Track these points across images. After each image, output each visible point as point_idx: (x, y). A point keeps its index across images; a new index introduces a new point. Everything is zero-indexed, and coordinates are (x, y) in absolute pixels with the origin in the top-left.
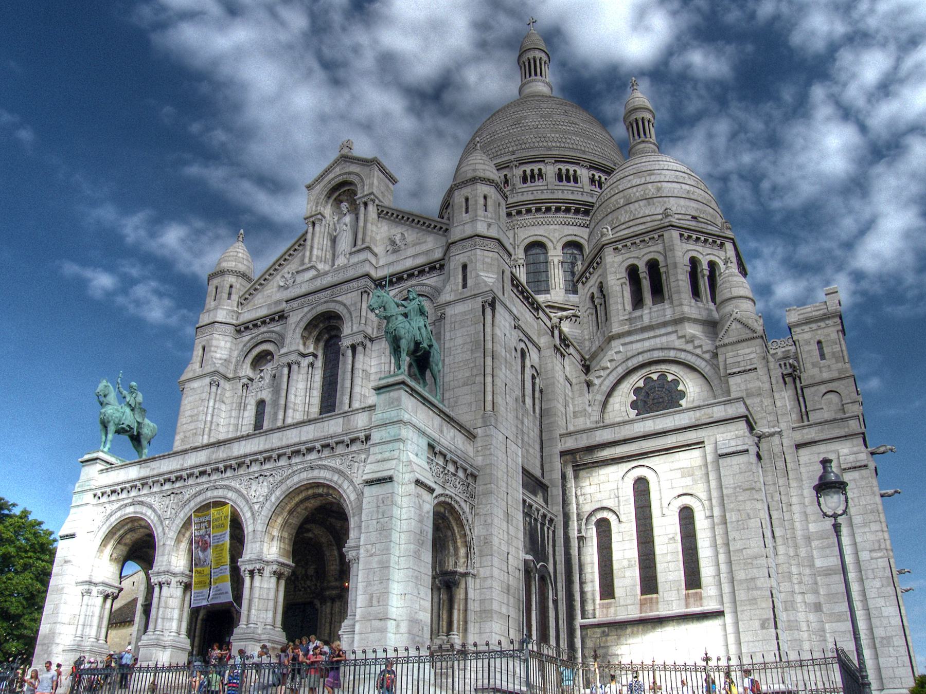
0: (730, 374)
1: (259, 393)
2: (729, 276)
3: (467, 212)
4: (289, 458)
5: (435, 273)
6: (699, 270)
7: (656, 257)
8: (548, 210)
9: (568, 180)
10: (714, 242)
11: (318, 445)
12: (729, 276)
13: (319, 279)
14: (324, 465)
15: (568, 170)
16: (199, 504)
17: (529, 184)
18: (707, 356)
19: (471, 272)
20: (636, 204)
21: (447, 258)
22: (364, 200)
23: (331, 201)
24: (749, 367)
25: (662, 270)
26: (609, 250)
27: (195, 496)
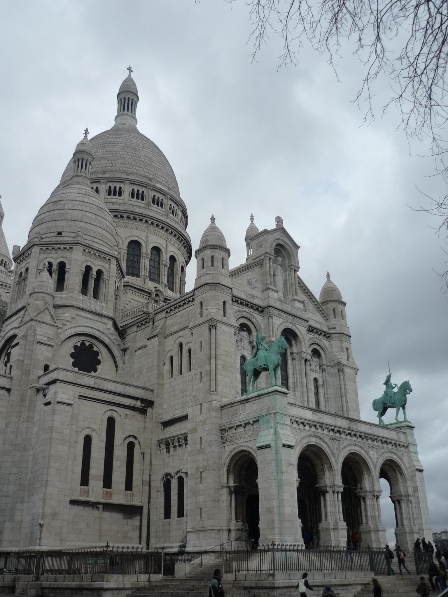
1: (243, 350)
4: (383, 443)
5: (325, 338)
11: (393, 442)
13: (285, 305)
21: (332, 335)
22: (296, 269)
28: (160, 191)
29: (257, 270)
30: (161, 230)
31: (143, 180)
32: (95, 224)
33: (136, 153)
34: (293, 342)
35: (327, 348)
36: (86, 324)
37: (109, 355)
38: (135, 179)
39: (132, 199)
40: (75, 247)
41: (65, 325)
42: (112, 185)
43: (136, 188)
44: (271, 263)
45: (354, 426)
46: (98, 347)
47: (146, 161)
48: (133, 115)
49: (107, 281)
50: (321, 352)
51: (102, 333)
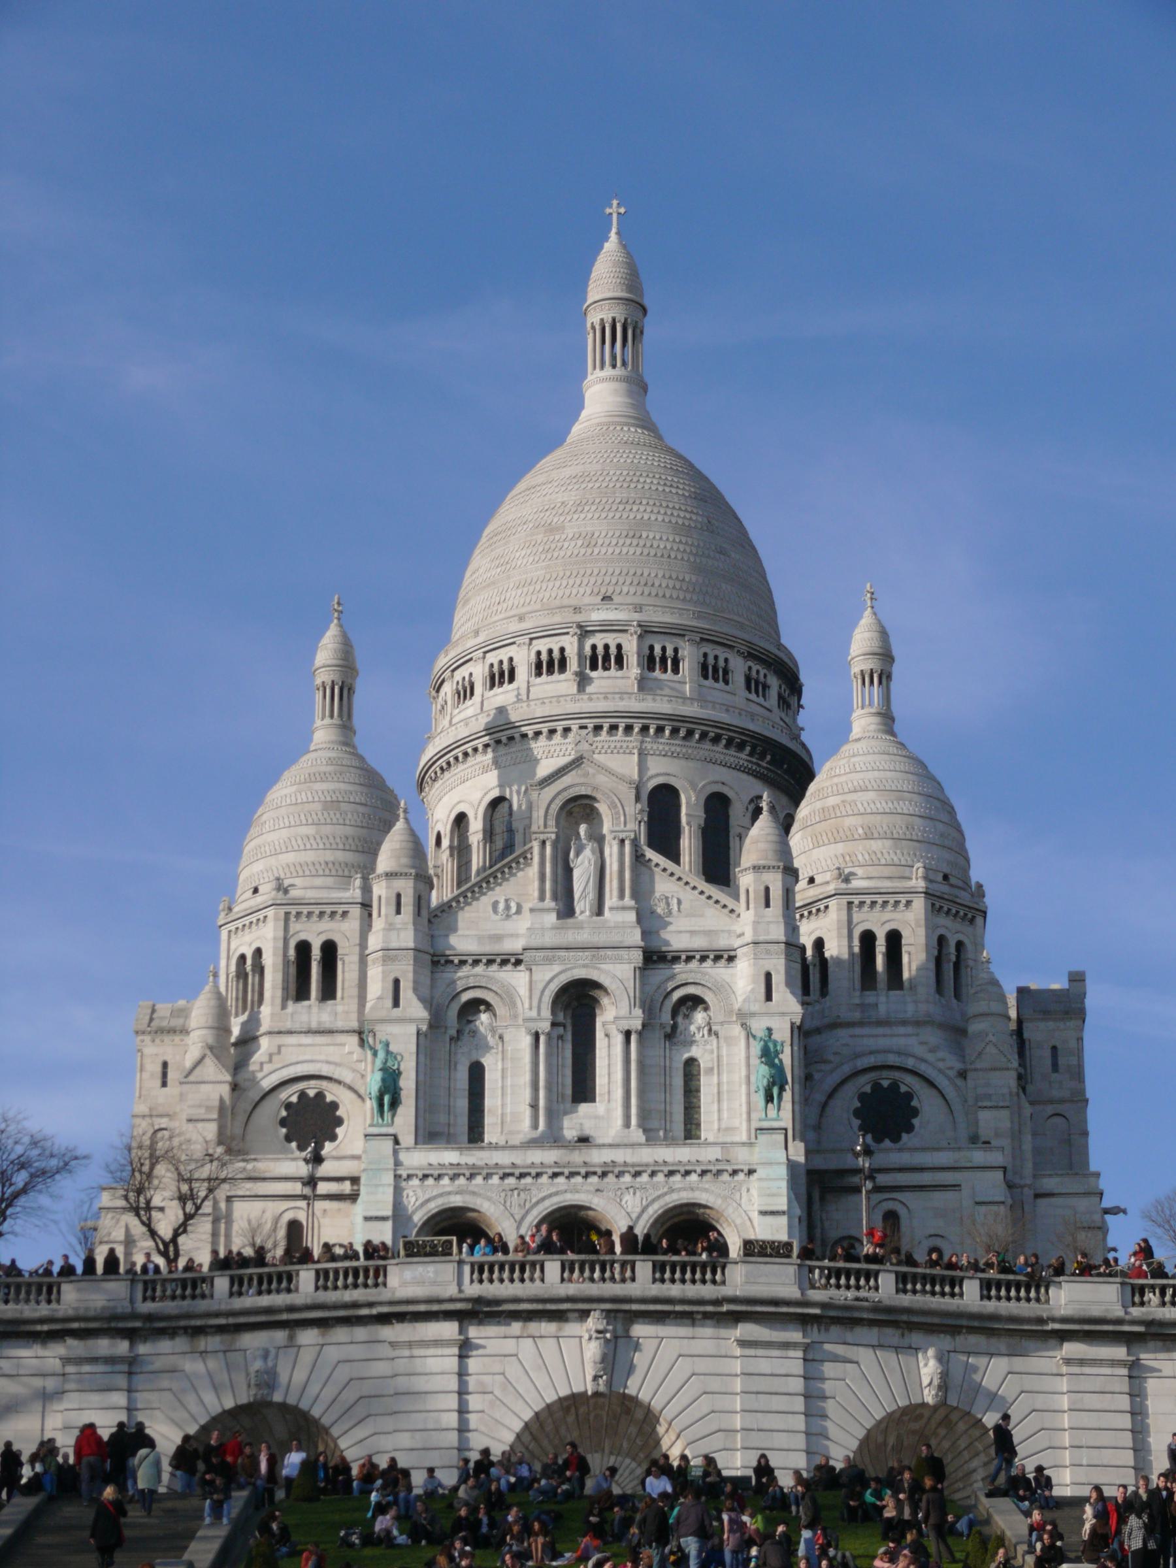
3: (767, 905)
6: (944, 951)
7: (900, 929)
8: (690, 733)
9: (716, 680)
10: (966, 915)
13: (570, 932)
15: (716, 657)
17: (657, 673)
18: (951, 1073)
19: (777, 984)
20: (880, 842)
21: (739, 952)
22: (622, 835)
24: (1001, 1104)
25: (904, 949)
27: (550, 1196)
28: (607, 628)
29: (520, 874)
31: (557, 619)
32: (315, 846)
34: (605, 1001)
36: (301, 1058)
37: (359, 1100)
38: (536, 625)
39: (539, 680)
42: (493, 658)
45: (577, 1157)
46: (333, 1093)
47: (576, 552)
49: (346, 958)
50: (708, 997)
51: (336, 1064)
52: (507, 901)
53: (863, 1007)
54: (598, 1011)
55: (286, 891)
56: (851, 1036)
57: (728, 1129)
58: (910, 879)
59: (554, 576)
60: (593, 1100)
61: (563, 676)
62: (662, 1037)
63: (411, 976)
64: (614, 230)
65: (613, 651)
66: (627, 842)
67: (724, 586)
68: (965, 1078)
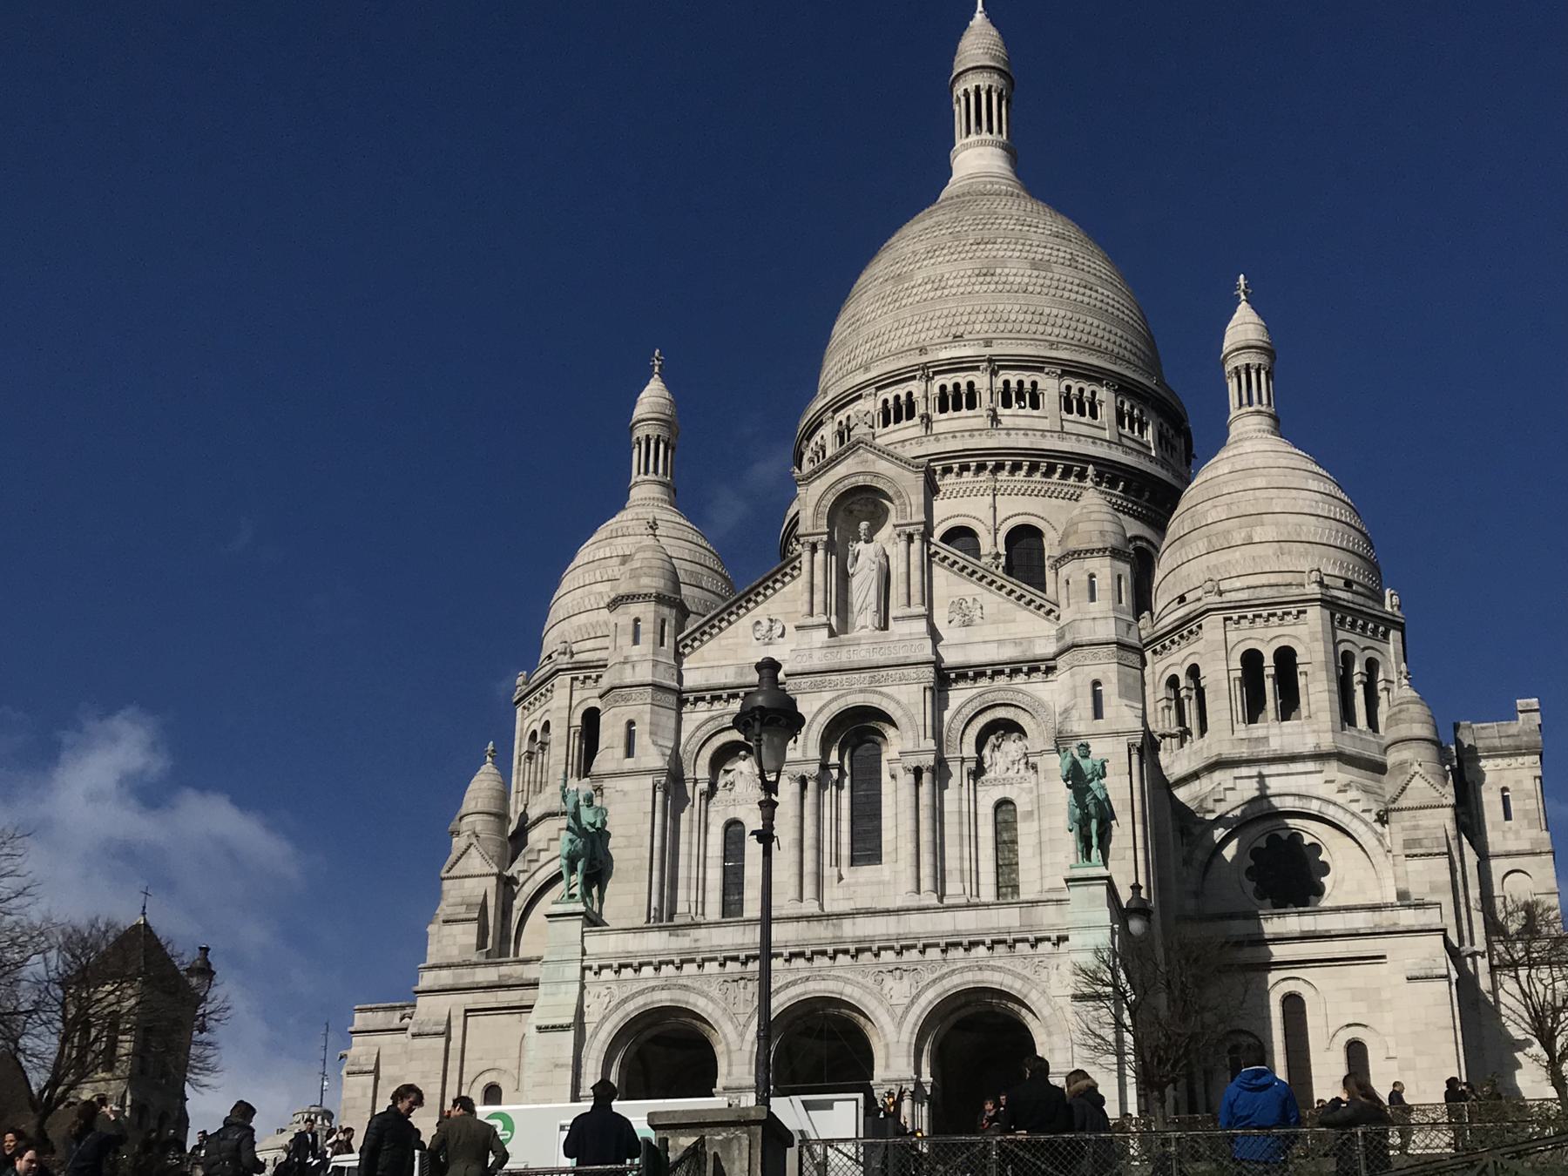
0: (1407, 856)
2: (1408, 702)
3: (1093, 599)
9: (1082, 413)
10: (1376, 628)
11: (988, 941)
12: (1408, 702)
14: (1001, 968)
15: (1081, 390)
16: (793, 998)
21: (1060, 662)
22: (909, 529)
23: (841, 514)
24: (1436, 851)
25: (1300, 669)
26: (1217, 618)
27: (787, 986)
28: (956, 366)
29: (785, 589)
30: (965, 473)
31: (902, 363)
33: (900, 287)
34: (890, 732)
35: (1042, 704)
39: (886, 430)
40: (557, 681)
41: (537, 861)
43: (889, 394)
44: (820, 555)
47: (924, 296)
48: (985, 136)
50: (1024, 720)
52: (771, 620)
53: (1249, 740)
54: (884, 748)
55: (572, 655)
56: (1236, 778)
57: (1051, 890)
58: (1303, 585)
59: (902, 324)
60: (881, 863)
61: (910, 423)
62: (965, 774)
63: (647, 718)
64: (980, 7)
65: (964, 387)
66: (916, 537)
67: (1090, 320)
68: (1387, 822)
